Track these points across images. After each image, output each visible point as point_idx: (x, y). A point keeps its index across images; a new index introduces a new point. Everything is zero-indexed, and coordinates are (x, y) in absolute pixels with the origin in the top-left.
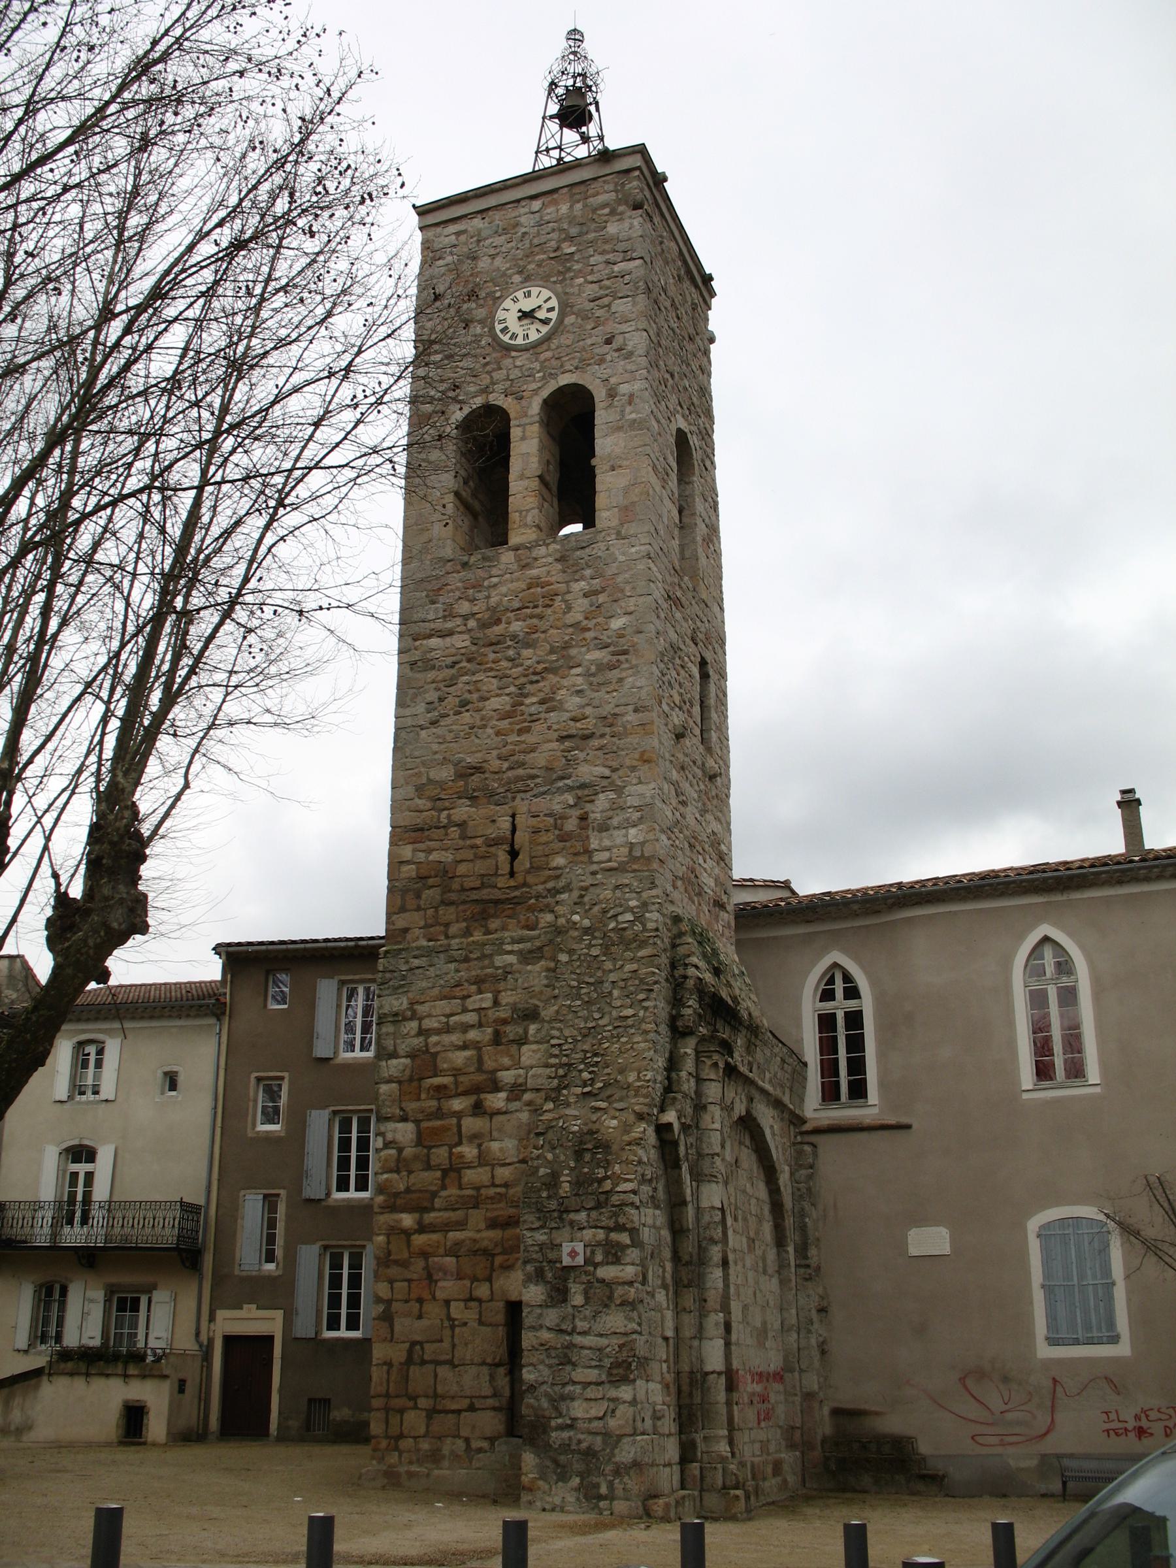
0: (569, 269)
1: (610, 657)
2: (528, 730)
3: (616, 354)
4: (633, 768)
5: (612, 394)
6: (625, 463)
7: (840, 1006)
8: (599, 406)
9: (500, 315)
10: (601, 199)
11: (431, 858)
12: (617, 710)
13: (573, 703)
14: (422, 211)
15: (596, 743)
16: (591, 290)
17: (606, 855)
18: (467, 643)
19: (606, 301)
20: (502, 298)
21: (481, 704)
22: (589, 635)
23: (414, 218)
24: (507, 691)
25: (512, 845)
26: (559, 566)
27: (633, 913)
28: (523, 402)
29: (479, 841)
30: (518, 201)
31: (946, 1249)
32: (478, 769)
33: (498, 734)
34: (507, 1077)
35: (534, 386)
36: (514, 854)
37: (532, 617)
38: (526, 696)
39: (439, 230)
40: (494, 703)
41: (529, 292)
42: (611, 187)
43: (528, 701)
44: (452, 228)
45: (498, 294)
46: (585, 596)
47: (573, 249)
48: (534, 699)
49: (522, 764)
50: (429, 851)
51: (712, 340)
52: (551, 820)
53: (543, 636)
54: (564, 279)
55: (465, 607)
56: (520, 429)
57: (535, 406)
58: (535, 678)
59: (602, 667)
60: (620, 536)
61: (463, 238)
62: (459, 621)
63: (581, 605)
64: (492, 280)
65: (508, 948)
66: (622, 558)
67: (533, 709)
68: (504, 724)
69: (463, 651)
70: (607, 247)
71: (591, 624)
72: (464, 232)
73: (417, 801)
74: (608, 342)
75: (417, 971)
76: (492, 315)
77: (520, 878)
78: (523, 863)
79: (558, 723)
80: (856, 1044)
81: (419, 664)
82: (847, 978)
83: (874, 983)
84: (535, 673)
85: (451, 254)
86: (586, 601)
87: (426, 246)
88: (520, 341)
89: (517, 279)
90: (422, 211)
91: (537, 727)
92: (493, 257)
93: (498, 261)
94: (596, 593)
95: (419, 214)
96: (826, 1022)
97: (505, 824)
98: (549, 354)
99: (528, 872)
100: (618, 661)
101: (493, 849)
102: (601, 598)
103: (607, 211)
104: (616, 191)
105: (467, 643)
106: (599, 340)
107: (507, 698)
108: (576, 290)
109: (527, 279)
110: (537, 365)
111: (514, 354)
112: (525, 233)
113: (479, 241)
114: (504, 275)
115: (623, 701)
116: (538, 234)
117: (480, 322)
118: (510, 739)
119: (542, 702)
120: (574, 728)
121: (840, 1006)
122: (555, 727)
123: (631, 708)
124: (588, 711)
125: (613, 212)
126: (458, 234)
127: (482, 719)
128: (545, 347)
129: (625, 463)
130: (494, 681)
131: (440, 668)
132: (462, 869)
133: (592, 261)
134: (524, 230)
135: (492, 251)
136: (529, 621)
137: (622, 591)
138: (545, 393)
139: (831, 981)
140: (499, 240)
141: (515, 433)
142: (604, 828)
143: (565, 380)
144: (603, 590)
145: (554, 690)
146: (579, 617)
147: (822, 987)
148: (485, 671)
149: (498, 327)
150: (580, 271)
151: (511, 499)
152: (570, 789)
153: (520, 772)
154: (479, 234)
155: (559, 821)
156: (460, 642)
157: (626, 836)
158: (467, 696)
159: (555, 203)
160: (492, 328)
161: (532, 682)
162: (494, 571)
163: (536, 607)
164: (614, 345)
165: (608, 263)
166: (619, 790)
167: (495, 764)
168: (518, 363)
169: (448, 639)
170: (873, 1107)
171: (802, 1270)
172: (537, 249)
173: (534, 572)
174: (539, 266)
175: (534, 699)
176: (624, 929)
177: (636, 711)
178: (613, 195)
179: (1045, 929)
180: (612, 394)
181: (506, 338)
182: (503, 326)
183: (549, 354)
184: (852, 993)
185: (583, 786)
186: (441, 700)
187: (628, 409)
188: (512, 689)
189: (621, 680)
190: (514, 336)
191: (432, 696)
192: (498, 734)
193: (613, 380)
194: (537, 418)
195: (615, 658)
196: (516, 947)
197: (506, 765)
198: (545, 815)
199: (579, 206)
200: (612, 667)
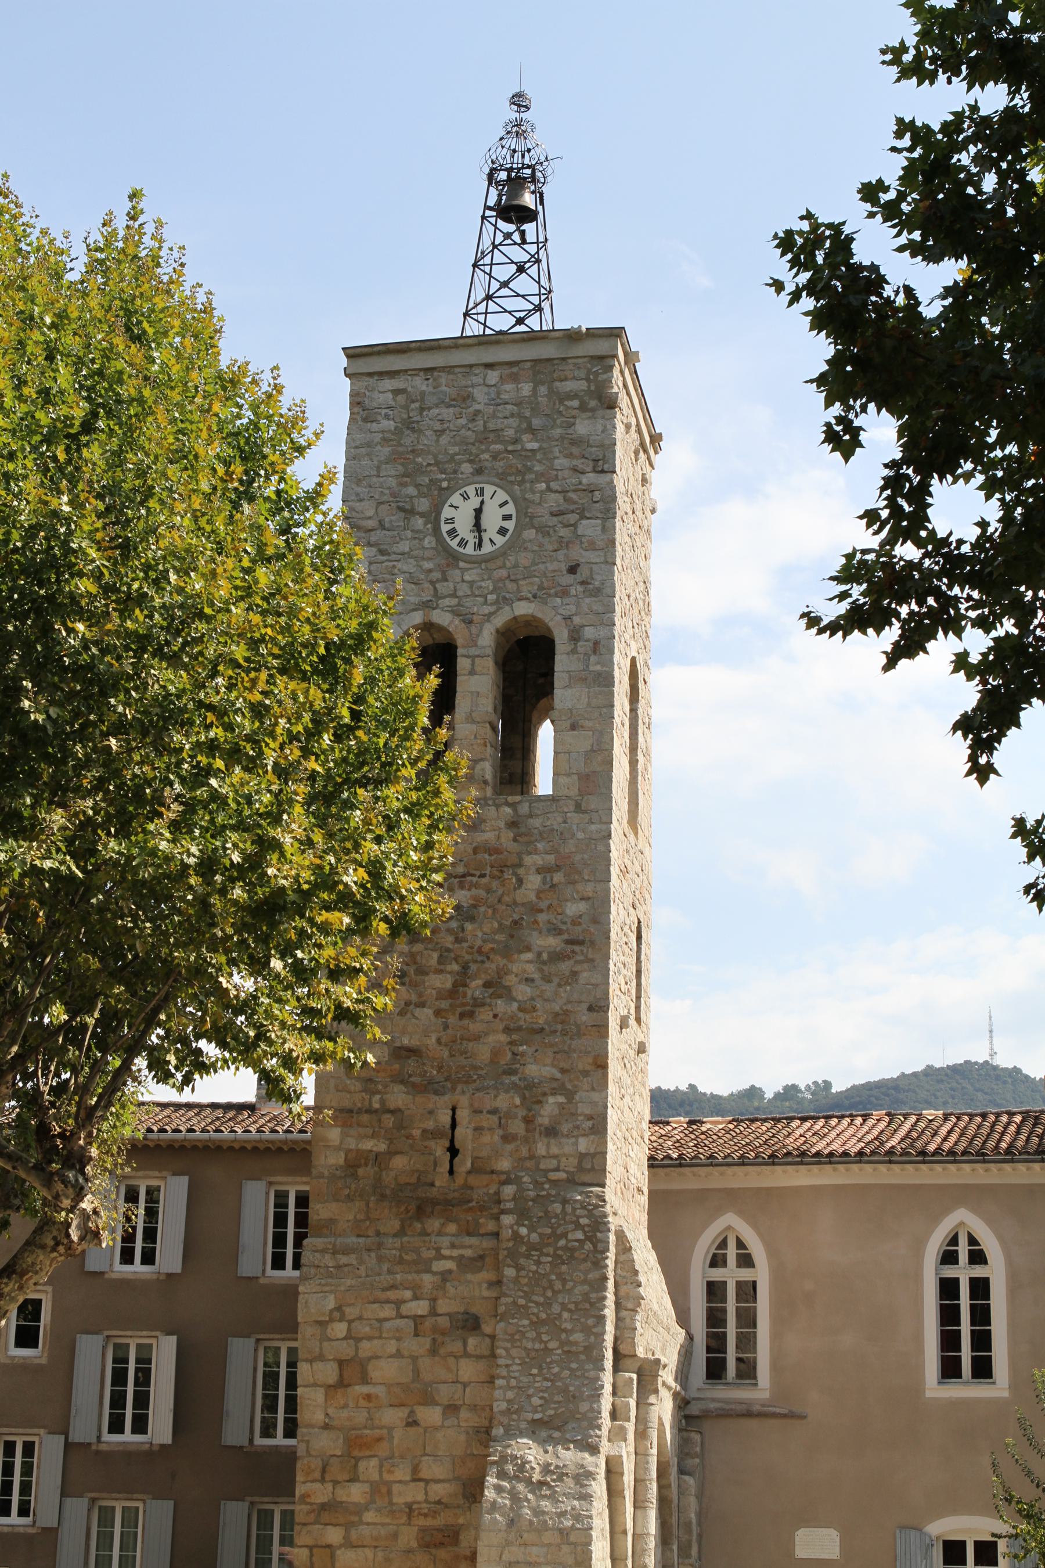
0: (530, 470)
2: (471, 1015)
3: (580, 588)
4: (586, 1073)
5: (575, 636)
6: (588, 724)
7: (731, 1275)
9: (447, 512)
10: (569, 386)
13: (523, 992)
14: (353, 354)
16: (554, 500)
17: (554, 1163)
19: (573, 518)
20: (450, 491)
22: (542, 918)
23: (344, 362)
24: (449, 968)
25: (452, 1141)
27: (585, 1232)
28: (474, 630)
32: (412, 1052)
34: (444, 1393)
35: (487, 609)
39: (372, 381)
41: (482, 489)
42: (582, 374)
44: (388, 384)
45: (445, 484)
46: (538, 871)
47: (535, 445)
52: (495, 1119)
54: (523, 481)
56: (469, 661)
57: (487, 638)
59: (557, 957)
60: (578, 808)
61: (401, 398)
63: (534, 881)
64: (437, 463)
66: (580, 835)
68: (444, 1004)
70: (575, 450)
71: (543, 905)
72: (403, 391)
74: (573, 570)
75: (346, 1269)
76: (437, 510)
77: (460, 1180)
78: (464, 1164)
82: (740, 1244)
83: (772, 1253)
85: (387, 417)
87: (356, 401)
88: (469, 550)
89: (467, 468)
90: (353, 354)
93: (444, 440)
95: (348, 356)
97: (445, 1119)
98: (504, 573)
99: (469, 1172)
100: (573, 952)
101: (432, 1144)
102: (558, 877)
103: (575, 403)
104: (588, 380)
108: (536, 497)
109: (479, 471)
110: (489, 585)
111: (462, 564)
112: (477, 412)
113: (422, 409)
114: (452, 459)
115: (575, 996)
116: (494, 416)
117: (422, 515)
123: (585, 1006)
125: (583, 408)
126: (396, 392)
128: (499, 562)
129: (588, 724)
134: (477, 407)
135: (438, 426)
136: (474, 891)
137: (580, 873)
139: (723, 1244)
140: (447, 413)
142: (551, 1132)
143: (523, 609)
144: (558, 868)
145: (502, 973)
146: (533, 897)
147: (713, 1251)
149: (445, 528)
150: (542, 475)
154: (422, 400)
157: (576, 1144)
159: (515, 378)
160: (437, 529)
163: (483, 876)
164: (579, 577)
165: (575, 470)
166: (570, 1096)
168: (467, 578)
170: (763, 1388)
172: (492, 436)
174: (495, 457)
177: (590, 1009)
178: (583, 385)
179: (963, 1218)
180: (575, 636)
181: (454, 543)
182: (449, 527)
183: (504, 573)
184: (746, 1261)
187: (593, 658)
188: (455, 967)
189: (574, 974)
190: (463, 543)
193: (577, 620)
194: (489, 651)
195: (569, 948)
196: (456, 1253)
198: (489, 1112)
199: (543, 390)
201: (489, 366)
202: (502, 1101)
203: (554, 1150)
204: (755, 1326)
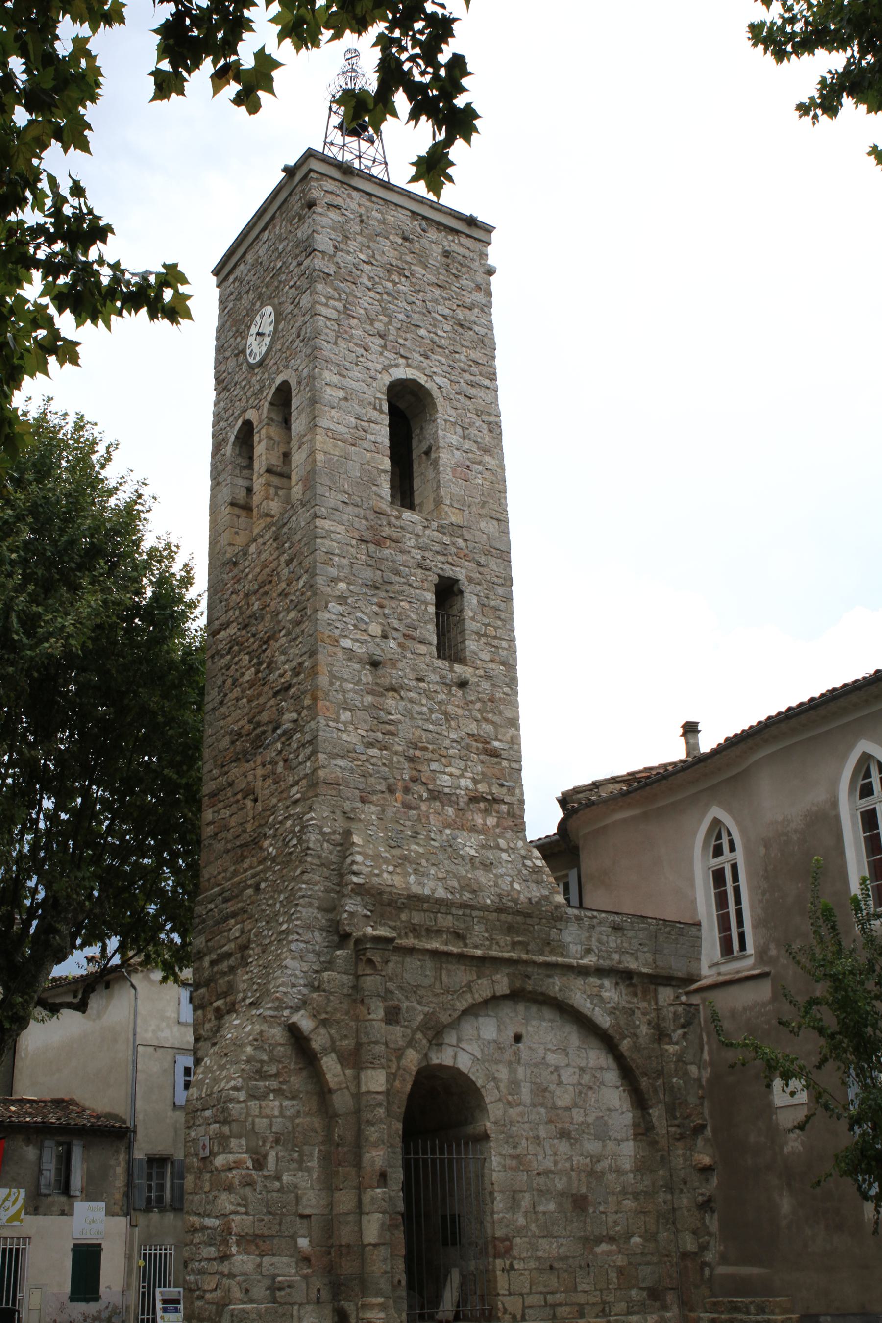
8: (294, 394)
12: (300, 660)
29: (239, 796)
30: (257, 237)
32: (239, 735)
36: (256, 800)
44: (231, 279)
50: (218, 812)
51: (490, 272)
65: (249, 882)
84: (265, 643)
92: (248, 292)
96: (719, 876)
108: (283, 299)
118: (254, 704)
119: (268, 667)
126: (234, 282)
130: (247, 657)
139: (719, 837)
143: (278, 381)
146: (283, 585)
149: (248, 352)
162: (247, 564)
176: (291, 853)
181: (251, 360)
185: (285, 733)
201: (264, 229)
203: (297, 778)
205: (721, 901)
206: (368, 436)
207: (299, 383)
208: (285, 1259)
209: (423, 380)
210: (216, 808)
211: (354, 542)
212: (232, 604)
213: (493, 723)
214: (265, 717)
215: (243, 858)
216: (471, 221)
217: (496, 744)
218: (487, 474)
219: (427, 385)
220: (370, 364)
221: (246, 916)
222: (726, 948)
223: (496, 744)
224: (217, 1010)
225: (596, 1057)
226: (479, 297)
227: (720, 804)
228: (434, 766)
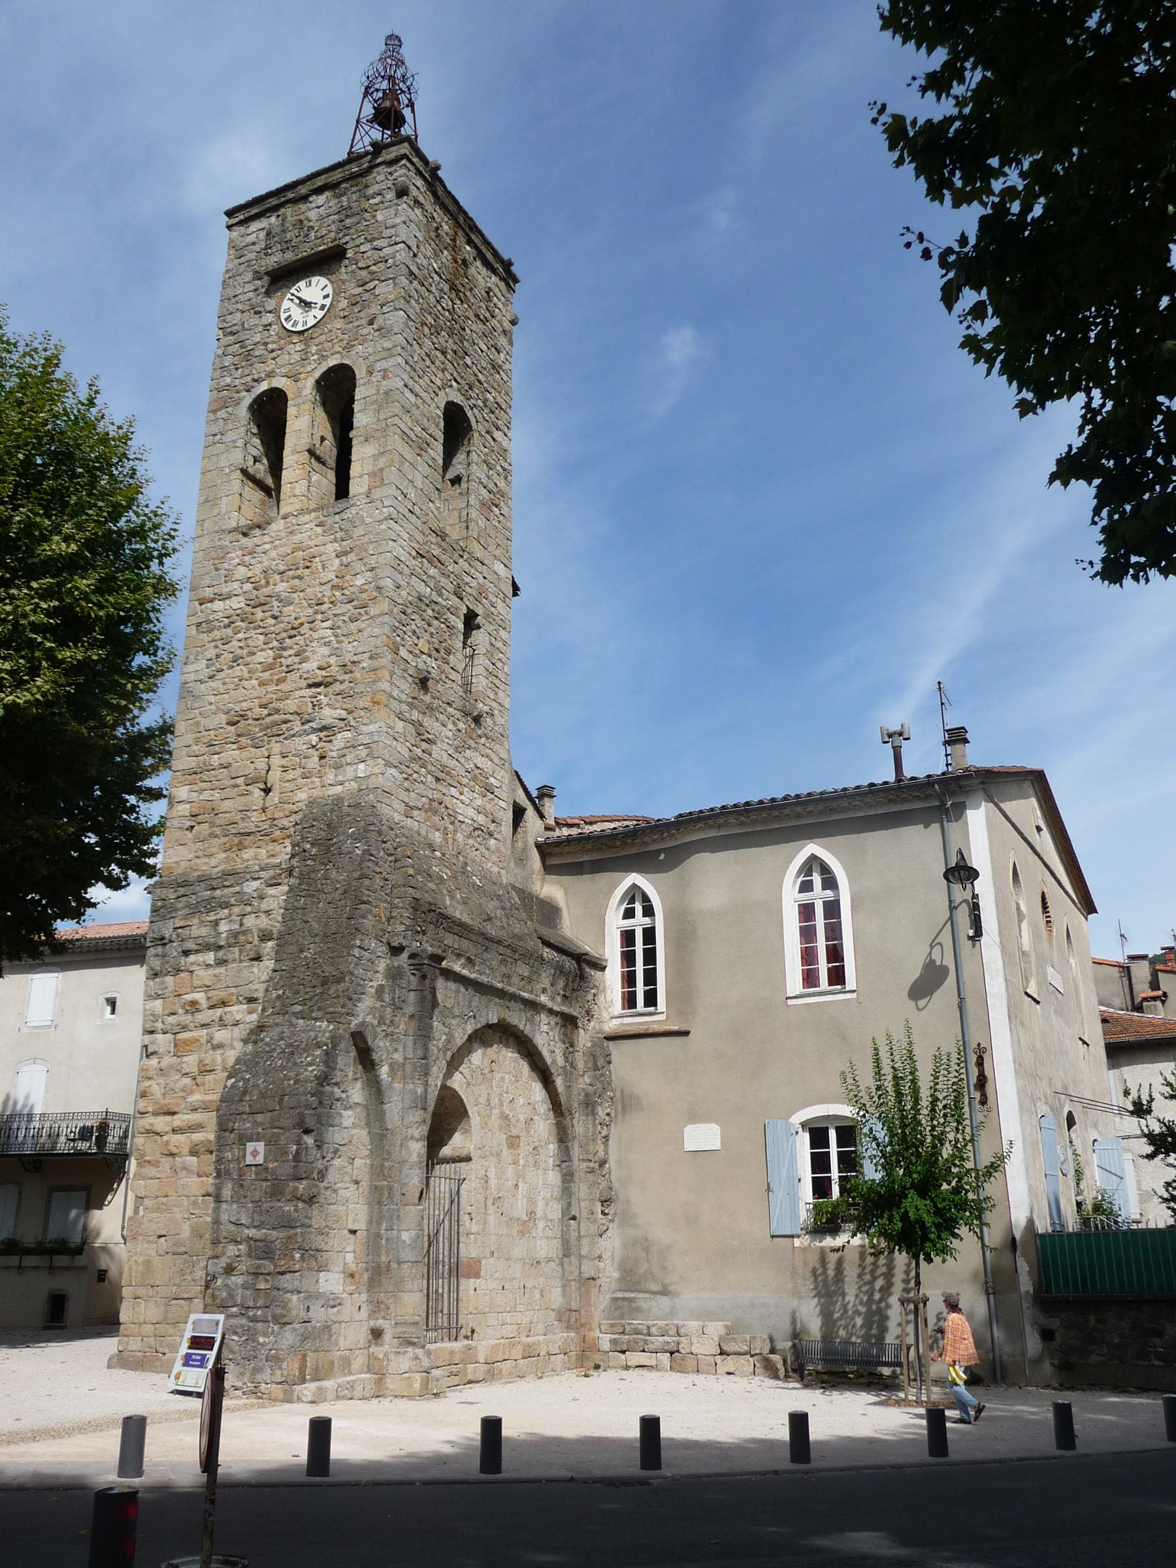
1: (353, 611)
2: (284, 680)
8: (359, 382)
11: (202, 797)
12: (355, 658)
15: (337, 687)
18: (243, 605)
19: (371, 285)
21: (249, 659)
24: (270, 646)
26: (319, 530)
29: (240, 781)
31: (716, 1145)
33: (261, 684)
36: (267, 791)
37: (294, 578)
38: (284, 649)
40: (260, 657)
43: (285, 654)
48: (292, 652)
49: (277, 711)
50: (202, 791)
52: (298, 760)
53: (301, 594)
55: (242, 572)
57: (308, 386)
58: (293, 632)
62: (236, 585)
67: (289, 661)
69: (238, 612)
73: (195, 748)
77: (269, 814)
79: (308, 672)
80: (650, 956)
81: (204, 625)
82: (645, 898)
84: (293, 628)
86: (337, 561)
91: (293, 676)
94: (345, 553)
96: (628, 937)
97: (261, 764)
102: (351, 557)
105: (243, 605)
106: (363, 322)
107: (270, 652)
115: (360, 650)
120: (320, 675)
121: (639, 922)
122: (305, 676)
124: (332, 660)
127: (249, 672)
130: (262, 638)
131: (219, 628)
132: (226, 805)
133: (363, 248)
137: (366, 550)
138: (317, 374)
141: (291, 411)
143: (333, 362)
147: (625, 905)
148: (255, 628)
149: (283, 316)
151: (284, 472)
152: (315, 730)
153: (276, 717)
155: (303, 761)
156: (237, 603)
157: (356, 770)
158: (239, 652)
161: (290, 637)
163: (297, 569)
164: (375, 326)
167: (258, 712)
169: (227, 601)
171: (585, 1164)
173: (298, 538)
175: (292, 652)
181: (289, 326)
182: (287, 315)
184: (649, 911)
185: (324, 728)
186: (218, 656)
188: (275, 644)
190: (295, 324)
191: (211, 653)
192: (261, 684)
197: (266, 712)
200: (353, 620)
202: (299, 744)
203: (340, 778)
204: (655, 964)
205: (628, 958)
206: (429, 450)
207: (370, 373)
208: (337, 1276)
209: (467, 409)
210: (195, 787)
211: (414, 553)
212: (237, 576)
213: (491, 760)
214: (291, 705)
215: (241, 847)
216: (507, 265)
217: (492, 780)
218: (501, 518)
219: (469, 414)
220: (433, 378)
221: (249, 909)
222: (630, 1001)
223: (492, 780)
224: (193, 1003)
225: (538, 1092)
226: (503, 341)
227: (639, 871)
228: (453, 791)
